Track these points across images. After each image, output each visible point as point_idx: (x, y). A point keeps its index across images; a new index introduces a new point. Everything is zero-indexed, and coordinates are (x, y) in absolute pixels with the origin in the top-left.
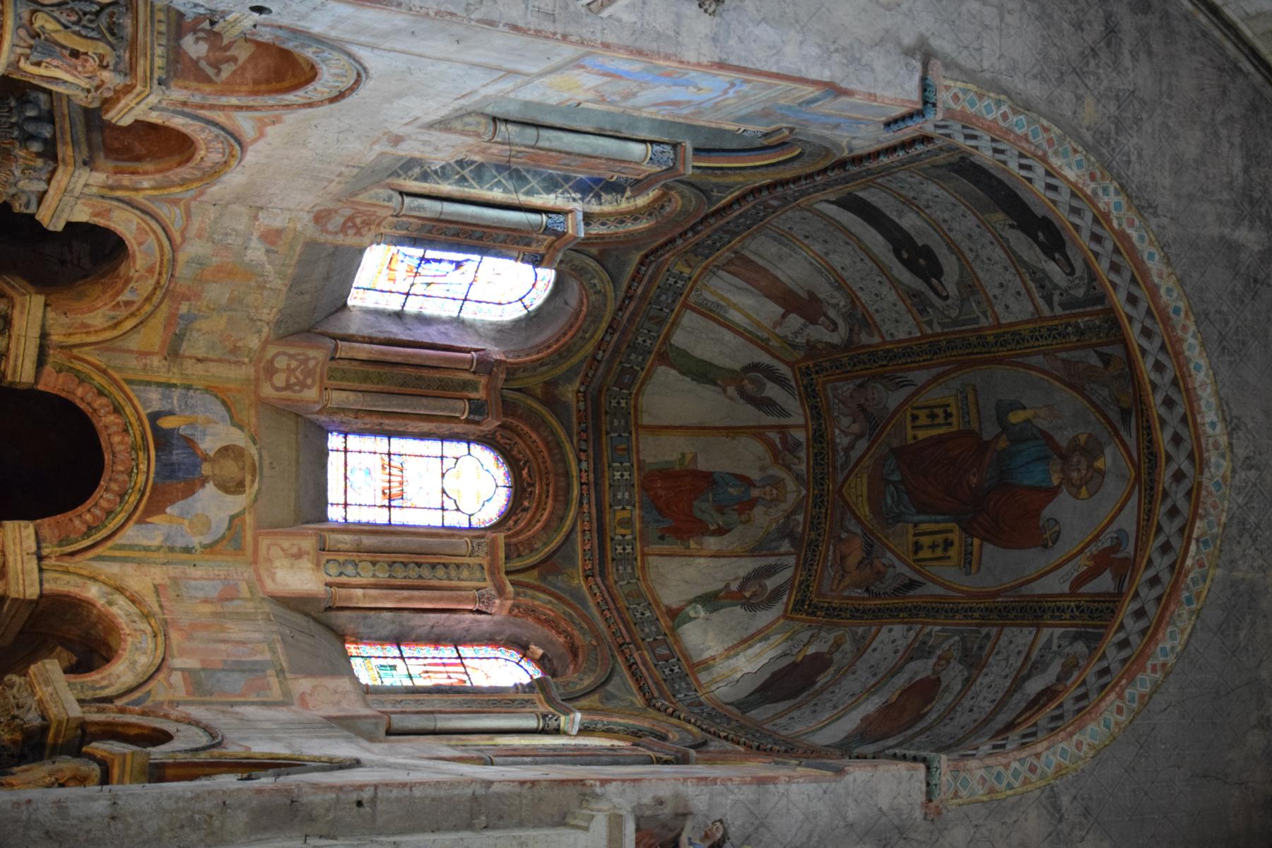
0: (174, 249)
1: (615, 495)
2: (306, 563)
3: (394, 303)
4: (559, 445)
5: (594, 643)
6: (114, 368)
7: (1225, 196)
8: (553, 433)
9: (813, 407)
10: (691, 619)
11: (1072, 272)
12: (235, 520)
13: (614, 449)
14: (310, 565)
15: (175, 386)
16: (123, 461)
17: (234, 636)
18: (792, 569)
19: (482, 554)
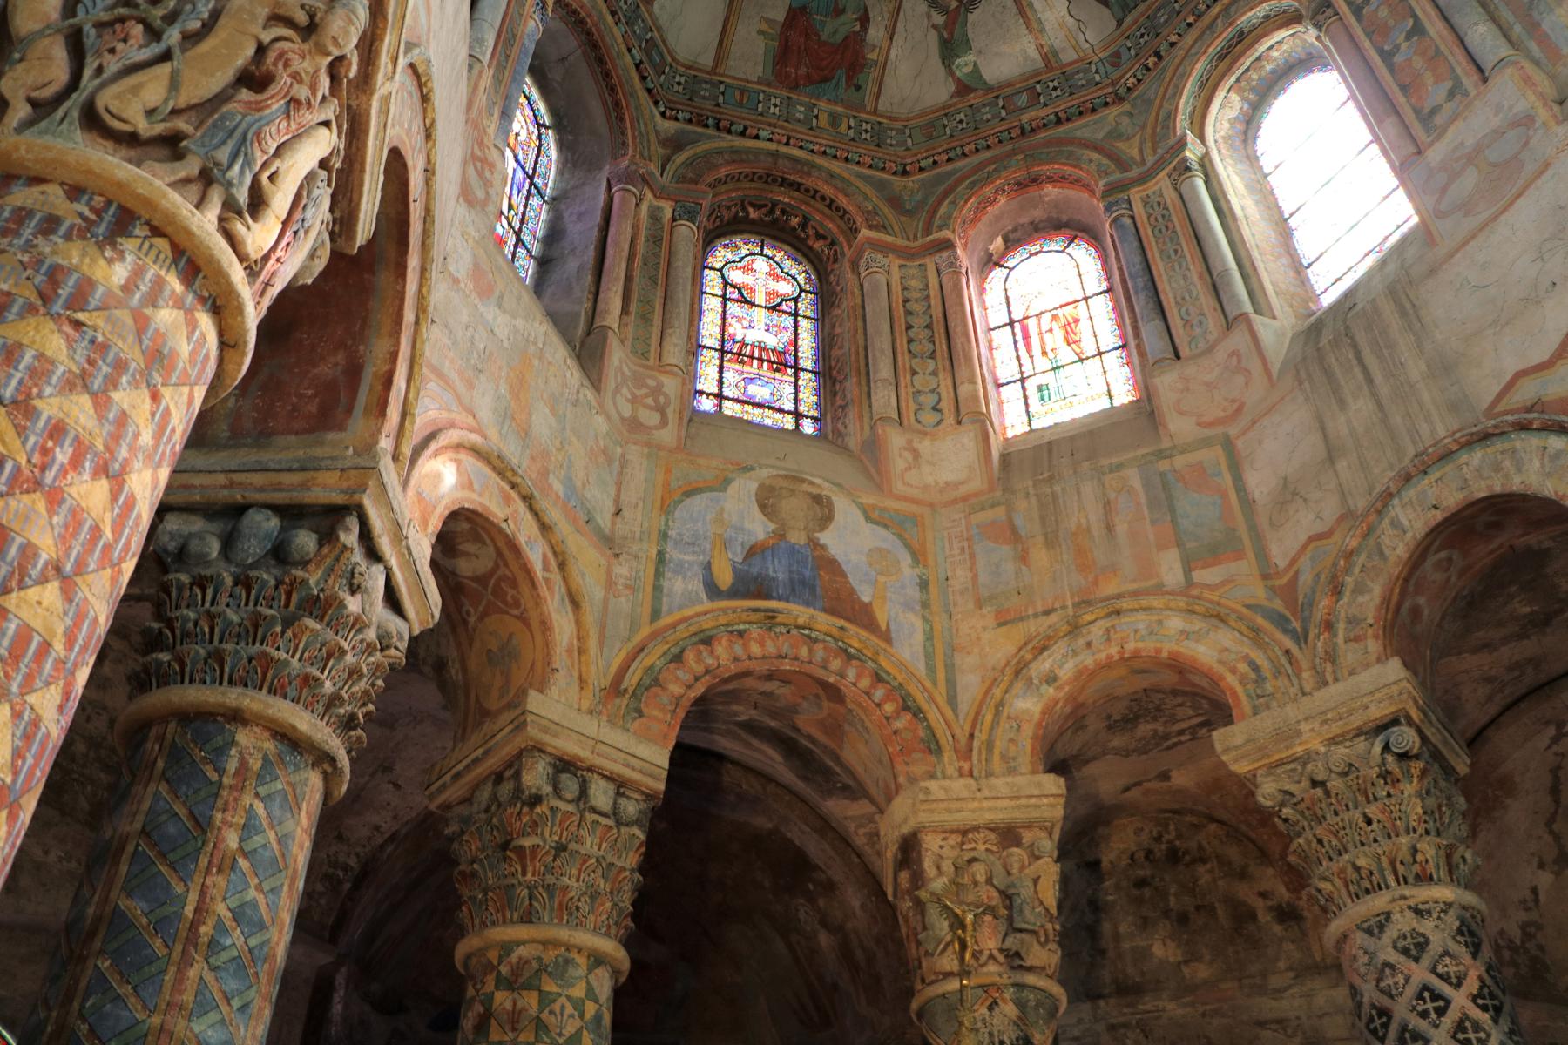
2: (925, 446)
6: (634, 626)
13: (741, 104)
15: (660, 554)
16: (792, 646)
17: (1094, 517)
19: (886, 261)
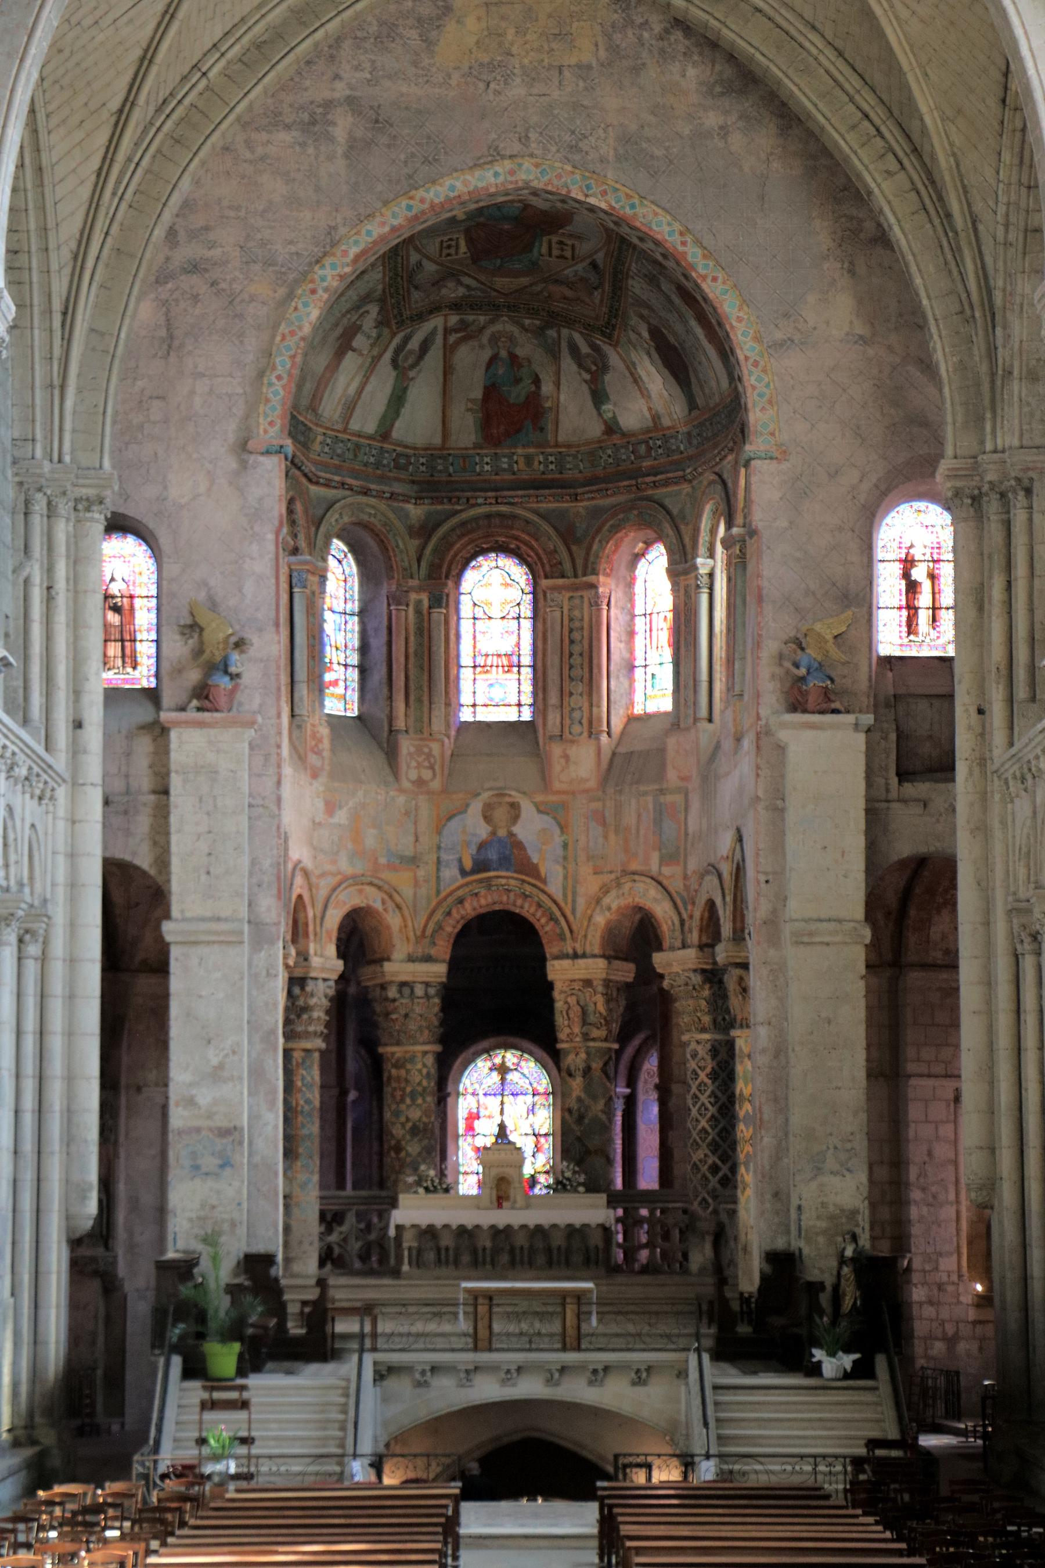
0: (346, 879)
1: (504, 470)
2: (573, 751)
3: (354, 675)
4: (463, 524)
5: (635, 512)
7: (311, 150)
8: (453, 530)
9: (431, 312)
10: (614, 417)
12: (541, 809)
13: (464, 470)
14: (574, 748)
17: (633, 821)
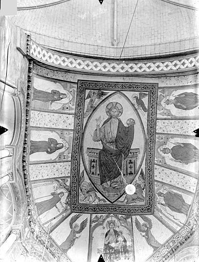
11: (66, 95)
18: (137, 216)
